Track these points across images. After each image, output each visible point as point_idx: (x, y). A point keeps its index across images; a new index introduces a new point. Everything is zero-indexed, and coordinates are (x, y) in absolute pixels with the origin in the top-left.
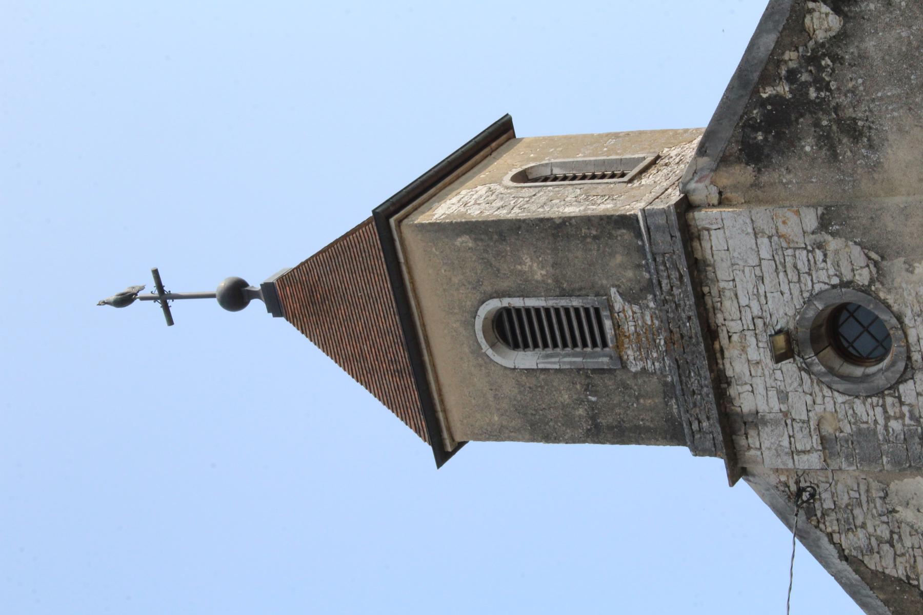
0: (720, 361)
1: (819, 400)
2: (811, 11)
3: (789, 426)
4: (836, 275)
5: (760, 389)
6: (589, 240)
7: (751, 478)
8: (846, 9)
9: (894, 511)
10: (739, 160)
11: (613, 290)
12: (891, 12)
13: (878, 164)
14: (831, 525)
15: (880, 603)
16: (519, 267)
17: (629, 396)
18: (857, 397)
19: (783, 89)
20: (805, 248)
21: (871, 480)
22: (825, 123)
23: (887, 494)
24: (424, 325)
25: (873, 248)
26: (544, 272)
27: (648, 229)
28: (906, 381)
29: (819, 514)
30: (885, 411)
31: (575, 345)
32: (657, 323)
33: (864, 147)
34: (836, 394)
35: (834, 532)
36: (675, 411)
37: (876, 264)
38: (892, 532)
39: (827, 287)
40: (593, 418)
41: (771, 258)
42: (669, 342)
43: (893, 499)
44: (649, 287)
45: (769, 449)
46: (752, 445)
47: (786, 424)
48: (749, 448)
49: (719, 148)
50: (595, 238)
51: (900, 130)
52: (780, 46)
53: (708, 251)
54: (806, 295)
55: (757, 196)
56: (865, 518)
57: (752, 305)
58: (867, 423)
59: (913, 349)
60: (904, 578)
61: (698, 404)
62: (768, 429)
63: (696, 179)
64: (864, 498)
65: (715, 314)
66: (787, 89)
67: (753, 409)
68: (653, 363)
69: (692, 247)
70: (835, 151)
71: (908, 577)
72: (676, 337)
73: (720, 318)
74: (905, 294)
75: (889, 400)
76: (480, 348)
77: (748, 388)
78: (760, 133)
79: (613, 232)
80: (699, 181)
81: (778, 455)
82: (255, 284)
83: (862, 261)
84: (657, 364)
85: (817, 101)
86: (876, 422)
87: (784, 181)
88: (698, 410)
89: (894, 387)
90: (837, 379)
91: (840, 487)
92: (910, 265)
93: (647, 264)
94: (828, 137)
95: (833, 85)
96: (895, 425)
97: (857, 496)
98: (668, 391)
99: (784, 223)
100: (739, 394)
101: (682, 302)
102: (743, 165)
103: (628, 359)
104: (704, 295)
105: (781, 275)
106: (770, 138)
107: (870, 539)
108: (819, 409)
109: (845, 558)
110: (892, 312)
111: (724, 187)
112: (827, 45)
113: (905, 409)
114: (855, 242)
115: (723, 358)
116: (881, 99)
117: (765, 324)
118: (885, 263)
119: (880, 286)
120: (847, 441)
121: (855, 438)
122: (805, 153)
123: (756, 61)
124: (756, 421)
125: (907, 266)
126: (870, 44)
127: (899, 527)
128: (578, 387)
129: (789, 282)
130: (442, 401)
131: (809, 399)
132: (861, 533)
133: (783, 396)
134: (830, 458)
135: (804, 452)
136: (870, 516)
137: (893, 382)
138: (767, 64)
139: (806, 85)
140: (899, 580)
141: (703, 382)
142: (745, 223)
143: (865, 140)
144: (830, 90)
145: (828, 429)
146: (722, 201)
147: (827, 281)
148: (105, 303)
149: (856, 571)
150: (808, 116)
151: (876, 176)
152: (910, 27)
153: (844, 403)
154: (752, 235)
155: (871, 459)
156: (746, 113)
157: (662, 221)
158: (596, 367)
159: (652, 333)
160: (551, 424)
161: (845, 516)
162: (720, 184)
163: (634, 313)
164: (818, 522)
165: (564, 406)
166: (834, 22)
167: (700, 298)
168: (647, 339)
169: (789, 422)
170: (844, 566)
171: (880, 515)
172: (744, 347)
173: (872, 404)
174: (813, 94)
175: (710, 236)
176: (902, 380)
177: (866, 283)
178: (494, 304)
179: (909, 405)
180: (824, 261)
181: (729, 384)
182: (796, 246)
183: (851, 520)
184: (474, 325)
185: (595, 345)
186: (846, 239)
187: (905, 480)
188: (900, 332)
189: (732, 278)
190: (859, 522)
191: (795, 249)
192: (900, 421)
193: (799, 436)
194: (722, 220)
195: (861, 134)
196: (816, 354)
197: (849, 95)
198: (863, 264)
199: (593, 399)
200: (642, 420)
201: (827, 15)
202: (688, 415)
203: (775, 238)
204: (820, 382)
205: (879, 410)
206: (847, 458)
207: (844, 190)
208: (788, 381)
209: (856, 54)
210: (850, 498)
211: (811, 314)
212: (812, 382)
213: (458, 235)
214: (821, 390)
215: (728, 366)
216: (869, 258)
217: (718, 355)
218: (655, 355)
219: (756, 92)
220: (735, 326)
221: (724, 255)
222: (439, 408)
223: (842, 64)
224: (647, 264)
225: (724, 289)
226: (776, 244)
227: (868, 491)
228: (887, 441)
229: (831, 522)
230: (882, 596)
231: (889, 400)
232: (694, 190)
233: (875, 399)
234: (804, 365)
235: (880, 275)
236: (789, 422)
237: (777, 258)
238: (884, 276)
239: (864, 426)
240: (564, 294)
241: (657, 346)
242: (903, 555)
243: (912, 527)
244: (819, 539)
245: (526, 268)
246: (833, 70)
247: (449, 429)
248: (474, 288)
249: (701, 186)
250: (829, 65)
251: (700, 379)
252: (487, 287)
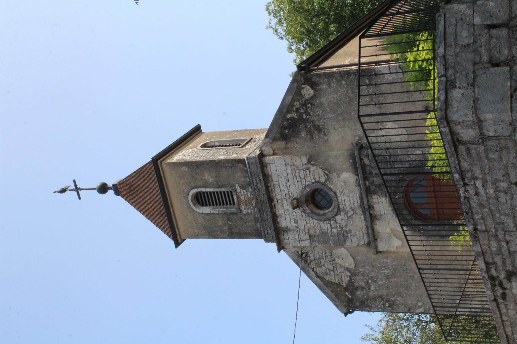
0: (274, 209)
1: (308, 222)
2: (303, 88)
3: (298, 232)
4: (314, 179)
5: (288, 219)
6: (228, 168)
7: (285, 250)
8: (315, 87)
9: (334, 260)
10: (279, 140)
11: (237, 185)
12: (331, 89)
13: (327, 140)
14: (313, 265)
15: (330, 292)
16: (204, 177)
17: (243, 222)
18: (321, 221)
19: (295, 115)
20: (303, 170)
21: (326, 249)
22: (309, 126)
23: (332, 254)
24: (170, 198)
25: (326, 169)
26: (212, 179)
27: (249, 164)
28: (338, 215)
29: (309, 261)
30: (331, 226)
31: (224, 204)
32: (252, 196)
33: (322, 135)
34: (314, 220)
35: (314, 268)
36: (259, 227)
37: (327, 175)
38: (334, 267)
39: (310, 183)
40: (230, 230)
41: (291, 173)
42: (257, 203)
43: (334, 256)
44: (249, 184)
45: (291, 239)
46: (286, 238)
47: (297, 231)
48: (285, 239)
49: (272, 135)
50: (230, 167)
51: (335, 129)
52: (293, 100)
53: (270, 171)
54: (303, 186)
55: (286, 152)
56: (324, 263)
58: (325, 230)
59: (340, 204)
60: (338, 283)
61: (267, 224)
62: (291, 233)
63: (265, 146)
64: (324, 256)
65: (272, 193)
66: (296, 115)
67: (286, 225)
68: (251, 211)
69: (264, 170)
70: (312, 136)
71: (339, 283)
72: (259, 201)
73: (274, 194)
74: (337, 185)
75: (332, 222)
76: (190, 206)
77: (284, 218)
78: (287, 130)
79: (236, 165)
80: (266, 147)
81: (295, 242)
82: (110, 184)
83: (322, 174)
84: (252, 211)
85: (306, 119)
86: (328, 229)
87: (295, 146)
88: (267, 227)
89: (334, 217)
90: (314, 215)
91: (316, 252)
92: (339, 175)
93: (248, 176)
94: (310, 131)
95: (311, 113)
96: (334, 230)
97: (322, 255)
98: (256, 220)
99: (296, 161)
101: (261, 189)
102: (281, 141)
103: (242, 209)
104: (268, 186)
105: (295, 179)
106: (290, 132)
107: (326, 270)
108: (308, 225)
109: (318, 276)
110: (333, 191)
111: (275, 149)
112: (309, 100)
113: (338, 225)
115: (275, 208)
116: (328, 118)
117: (289, 196)
118: (330, 174)
119: (329, 183)
120: (318, 236)
121: (321, 235)
122: (302, 137)
123: (285, 105)
124: (287, 230)
125: (338, 176)
126: (324, 99)
127: (336, 265)
128: (225, 219)
129: (298, 182)
130: (177, 225)
131: (305, 222)
132: (323, 268)
133: (296, 221)
134: (312, 242)
135: (304, 240)
136: (326, 262)
138: (289, 107)
139: (302, 113)
140: (336, 283)
141: (269, 217)
142: (282, 161)
143: (323, 132)
144: (310, 115)
145: (312, 232)
146: (274, 154)
148: (56, 192)
149: (322, 281)
150: (303, 124)
151: (327, 145)
152: (337, 94)
153: (317, 223)
154: (285, 166)
155: (326, 242)
156: (282, 123)
157: (253, 161)
158: (231, 212)
159: (250, 200)
160: (216, 232)
161: (318, 262)
162: (273, 148)
163: (244, 193)
164: (309, 264)
165: (220, 226)
166: (311, 92)
167: (267, 187)
168: (249, 202)
169: (298, 230)
170: (318, 279)
171: (330, 261)
173: (326, 223)
174: (305, 117)
175: (270, 166)
176: (336, 215)
177: (324, 182)
178: (195, 191)
179: (339, 223)
181: (277, 217)
183: (320, 264)
184: (188, 198)
185: (230, 204)
187: (338, 249)
188: (336, 198)
189: (278, 180)
190: (322, 264)
191: (299, 170)
192: (336, 229)
193: (302, 235)
194: (274, 160)
195: (321, 130)
196: (307, 206)
197: (317, 117)
199: (230, 223)
200: (248, 230)
201: (309, 89)
202: (263, 228)
203: (293, 166)
204: (309, 216)
205: (329, 225)
206: (318, 242)
207: (316, 150)
208: (298, 216)
209: (319, 103)
210: (319, 256)
211: (305, 192)
212: (306, 216)
213: (182, 167)
214: (309, 219)
215: (277, 211)
216: (325, 173)
217: (274, 207)
218: (252, 207)
219: (285, 116)
220: (279, 197)
221: (275, 172)
222: (176, 227)
223: (314, 106)
224: (248, 176)
225: (275, 184)
226: (293, 168)
227: (325, 253)
228: (332, 236)
229: (313, 264)
230: (330, 289)
232: (264, 150)
233: (327, 222)
234: (303, 210)
235: (328, 179)
236: (298, 230)
237: (293, 173)
238: (330, 179)
239: (324, 231)
240: (219, 187)
241: (252, 204)
242: (338, 275)
243: (340, 265)
244: (309, 270)
245: (206, 178)
246: (311, 108)
247: (180, 235)
248: (188, 185)
249: (267, 148)
250: (310, 107)
251: (267, 216)
252: (192, 185)
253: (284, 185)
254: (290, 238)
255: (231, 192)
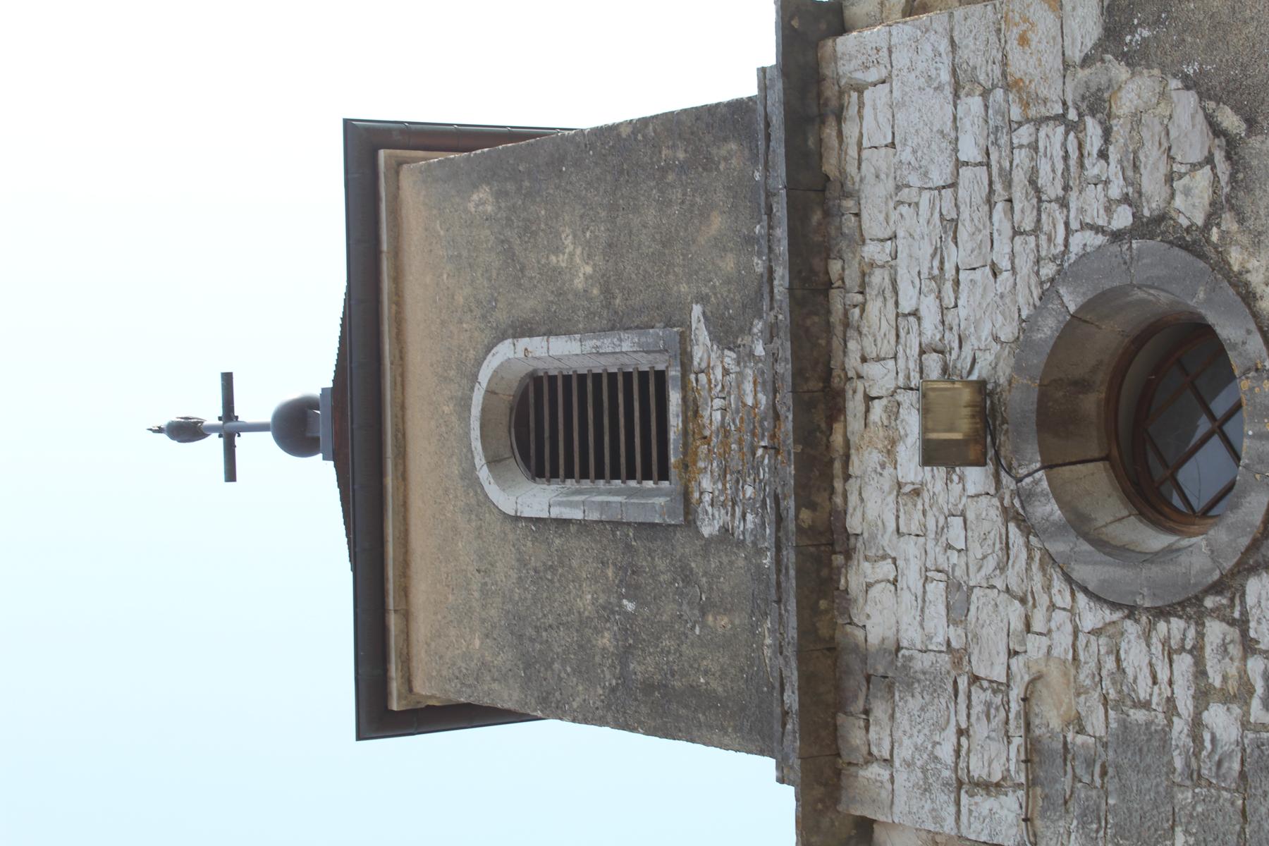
0: (838, 485)
3: (962, 698)
4: (1126, 199)
5: (912, 578)
6: (671, 177)
11: (697, 310)
18: (1132, 612)
26: (589, 270)
30: (1200, 672)
34: (1082, 598)
37: (1232, 147)
45: (909, 764)
48: (870, 758)
50: (683, 168)
53: (853, 152)
54: (1048, 270)
57: (923, 312)
58: (1146, 705)
62: (914, 704)
67: (890, 634)
68: (744, 517)
73: (853, 362)
75: (1215, 630)
84: (749, 517)
90: (1085, 547)
96: (1220, 720)
100: (869, 586)
103: (700, 501)
104: (829, 284)
114: (1185, 78)
115: (847, 477)
118: (1255, 142)
119: (1234, 227)
120: (1090, 763)
130: (405, 591)
131: (1015, 612)
137: (1228, 565)
147: (1101, 222)
148: (151, 430)
153: (1097, 632)
154: (948, 91)
160: (556, 666)
165: (583, 622)
169: (963, 683)
172: (893, 443)
173: (1165, 642)
175: (861, 105)
177: (1199, 220)
180: (1103, 155)
181: (848, 555)
182: (1044, 112)
186: (1163, 68)
189: (888, 233)
191: (1040, 122)
193: (980, 730)
194: (890, 52)
196: (1048, 466)
198: (1197, 155)
200: (706, 673)
203: (999, 94)
204: (1049, 559)
205: (1184, 663)
208: (977, 551)
211: (1048, 329)
212: (1030, 558)
214: (1048, 588)
215: (853, 499)
216: (1216, 130)
217: (837, 465)
218: (749, 491)
220: (881, 377)
228: (1194, 776)
231: (1215, 630)
233: (1177, 624)
236: (963, 683)
237: (994, 157)
238: (1249, 191)
240: (616, 325)
245: (561, 261)
247: (406, 661)
252: (501, 316)
253: (924, 275)
254: (902, 753)
255: (661, 376)
